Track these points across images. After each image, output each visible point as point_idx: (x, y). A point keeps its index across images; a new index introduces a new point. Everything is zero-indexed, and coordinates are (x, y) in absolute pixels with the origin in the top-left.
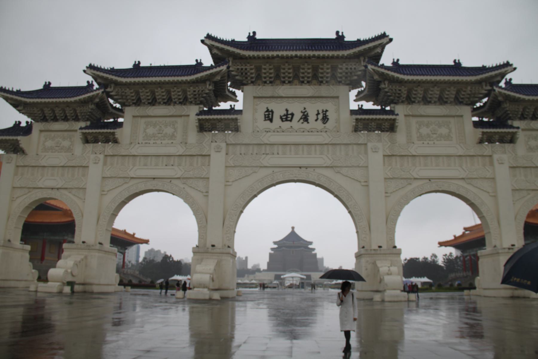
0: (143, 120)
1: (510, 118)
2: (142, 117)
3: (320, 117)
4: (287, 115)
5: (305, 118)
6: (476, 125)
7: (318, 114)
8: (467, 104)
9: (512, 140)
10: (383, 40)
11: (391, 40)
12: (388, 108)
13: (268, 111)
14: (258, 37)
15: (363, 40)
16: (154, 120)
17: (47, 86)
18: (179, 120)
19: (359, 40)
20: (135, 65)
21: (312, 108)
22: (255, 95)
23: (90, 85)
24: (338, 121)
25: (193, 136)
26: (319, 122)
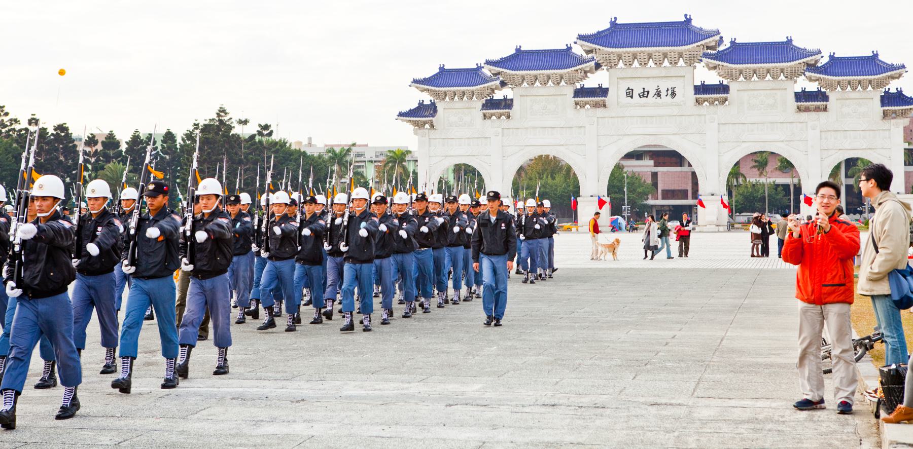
0: (529, 98)
3: (670, 92)
5: (658, 94)
9: (825, 109)
12: (725, 83)
14: (618, 22)
16: (538, 98)
17: (442, 69)
18: (559, 98)
19: (701, 29)
20: (517, 50)
23: (479, 68)
26: (669, 96)
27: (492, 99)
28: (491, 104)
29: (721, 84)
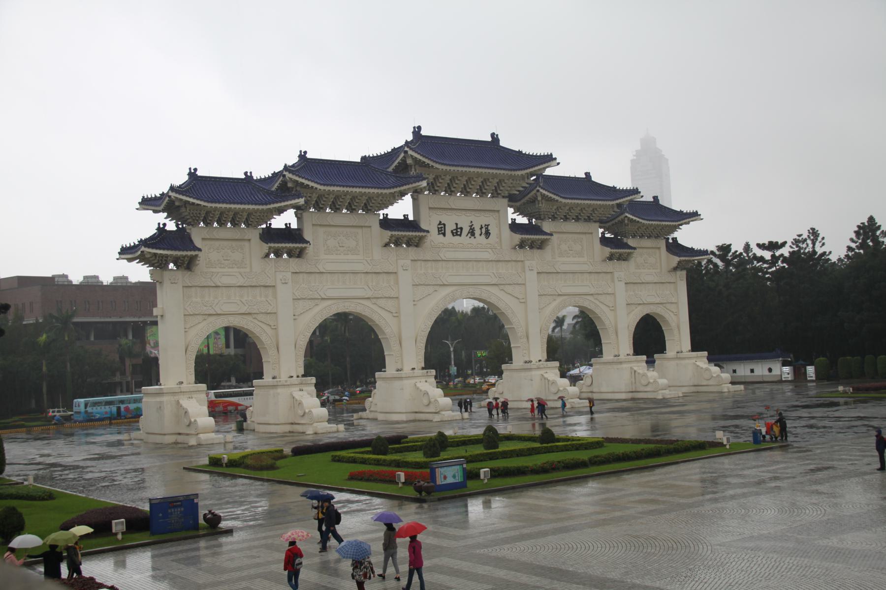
0: (321, 230)
1: (625, 237)
2: (320, 225)
3: (484, 230)
4: (457, 228)
5: (472, 232)
6: (604, 241)
7: (482, 228)
8: (595, 222)
10: (548, 159)
11: (558, 164)
13: (440, 223)
15: (525, 154)
18: (359, 231)
19: (520, 152)
21: (479, 221)
22: (431, 206)
24: (499, 236)
25: (378, 253)
26: (483, 236)
27: (269, 228)
28: (270, 235)
29: (530, 223)
